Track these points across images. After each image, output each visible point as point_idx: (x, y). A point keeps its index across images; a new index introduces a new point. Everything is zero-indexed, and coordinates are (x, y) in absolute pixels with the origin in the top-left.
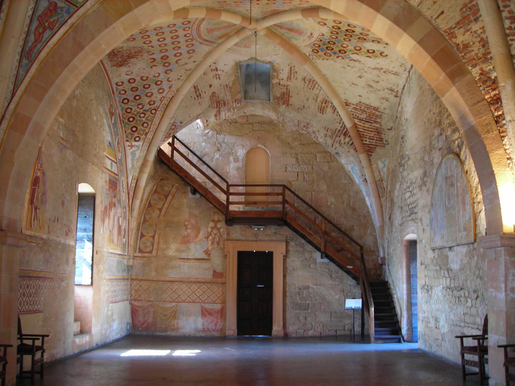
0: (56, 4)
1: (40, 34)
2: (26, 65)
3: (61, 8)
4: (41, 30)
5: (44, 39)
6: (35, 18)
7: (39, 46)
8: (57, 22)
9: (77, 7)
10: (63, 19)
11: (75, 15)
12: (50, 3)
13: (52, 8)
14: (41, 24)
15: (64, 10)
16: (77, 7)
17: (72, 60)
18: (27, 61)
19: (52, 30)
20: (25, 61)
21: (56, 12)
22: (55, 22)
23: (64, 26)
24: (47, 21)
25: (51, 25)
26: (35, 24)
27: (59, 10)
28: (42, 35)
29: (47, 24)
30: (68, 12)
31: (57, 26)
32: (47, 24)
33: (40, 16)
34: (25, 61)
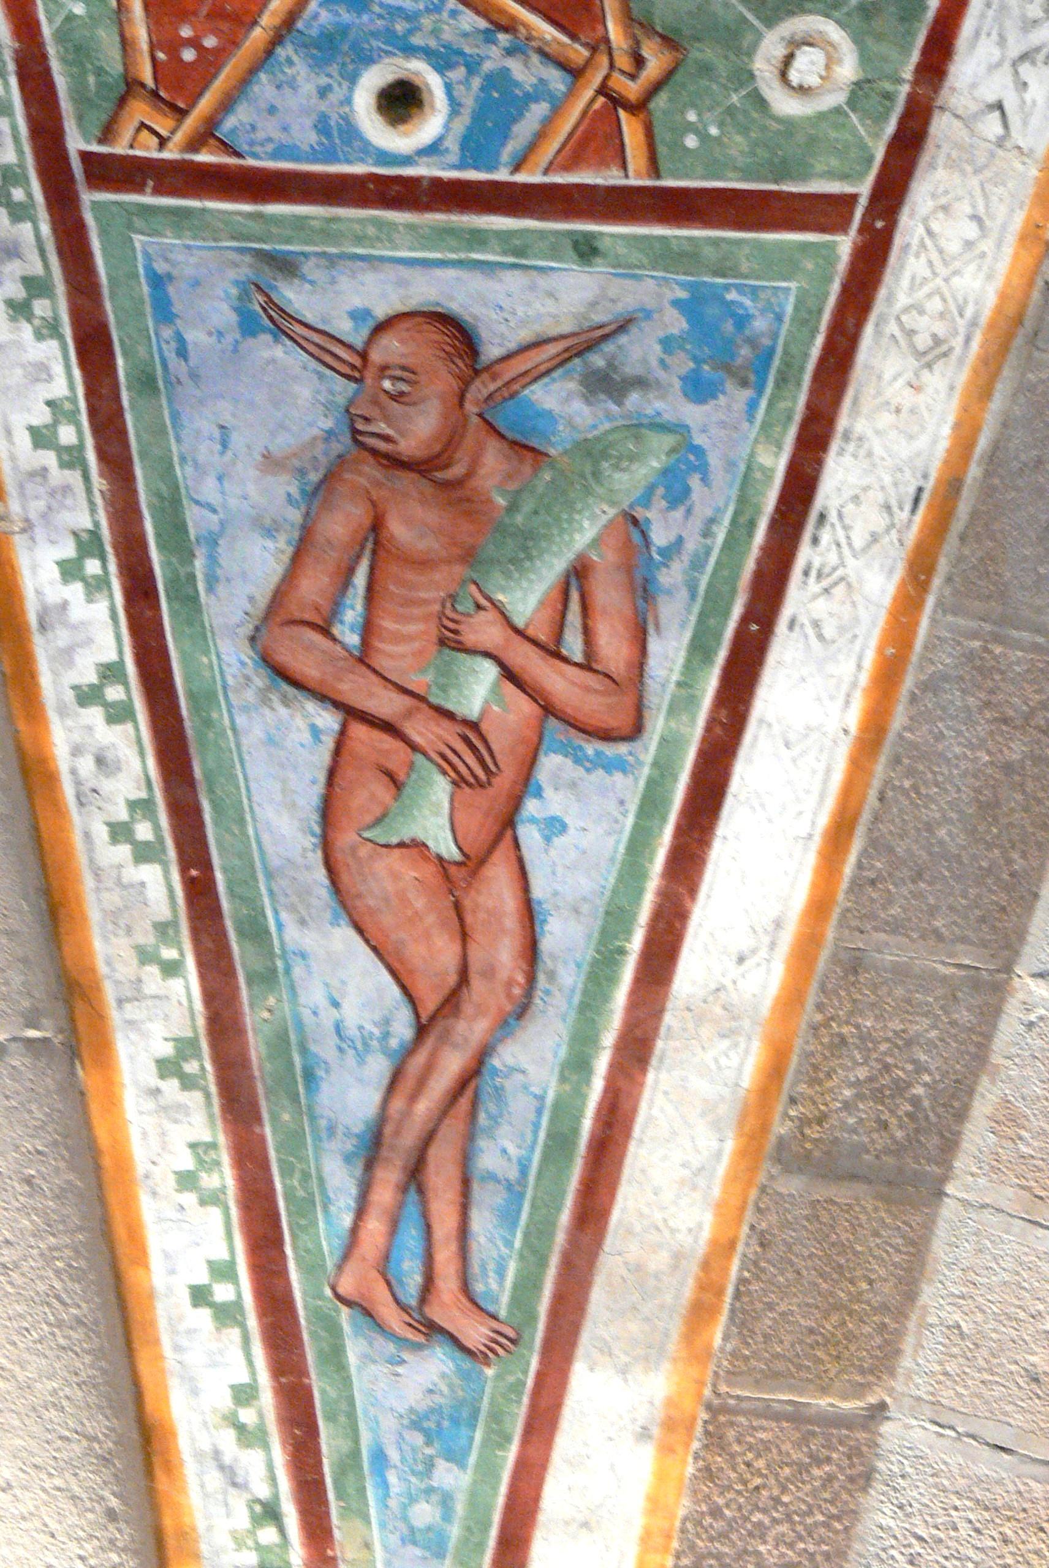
0: (456, 334)
1: (456, 877)
2: (438, 1428)
3: (582, 348)
4: (433, 816)
5: (565, 937)
6: (218, 655)
7: (532, 1060)
8: (643, 593)
9: (827, 212)
10: (712, 498)
11: (879, 359)
12: (357, 365)
13: (419, 429)
14: (370, 745)
15: (638, 351)
16: (827, 212)
17: (991, 992)
18: (432, 1369)
19: (635, 731)
20: (387, 1387)
21: (526, 451)
22: (608, 594)
23: (799, 598)
24: (451, 641)
25: (559, 682)
26: (275, 761)
27: (559, 403)
28: (496, 890)
29: (477, 689)
30: (722, 358)
31: (667, 654)
32: (477, 689)
33: (277, 610)
34: (387, 1387)
